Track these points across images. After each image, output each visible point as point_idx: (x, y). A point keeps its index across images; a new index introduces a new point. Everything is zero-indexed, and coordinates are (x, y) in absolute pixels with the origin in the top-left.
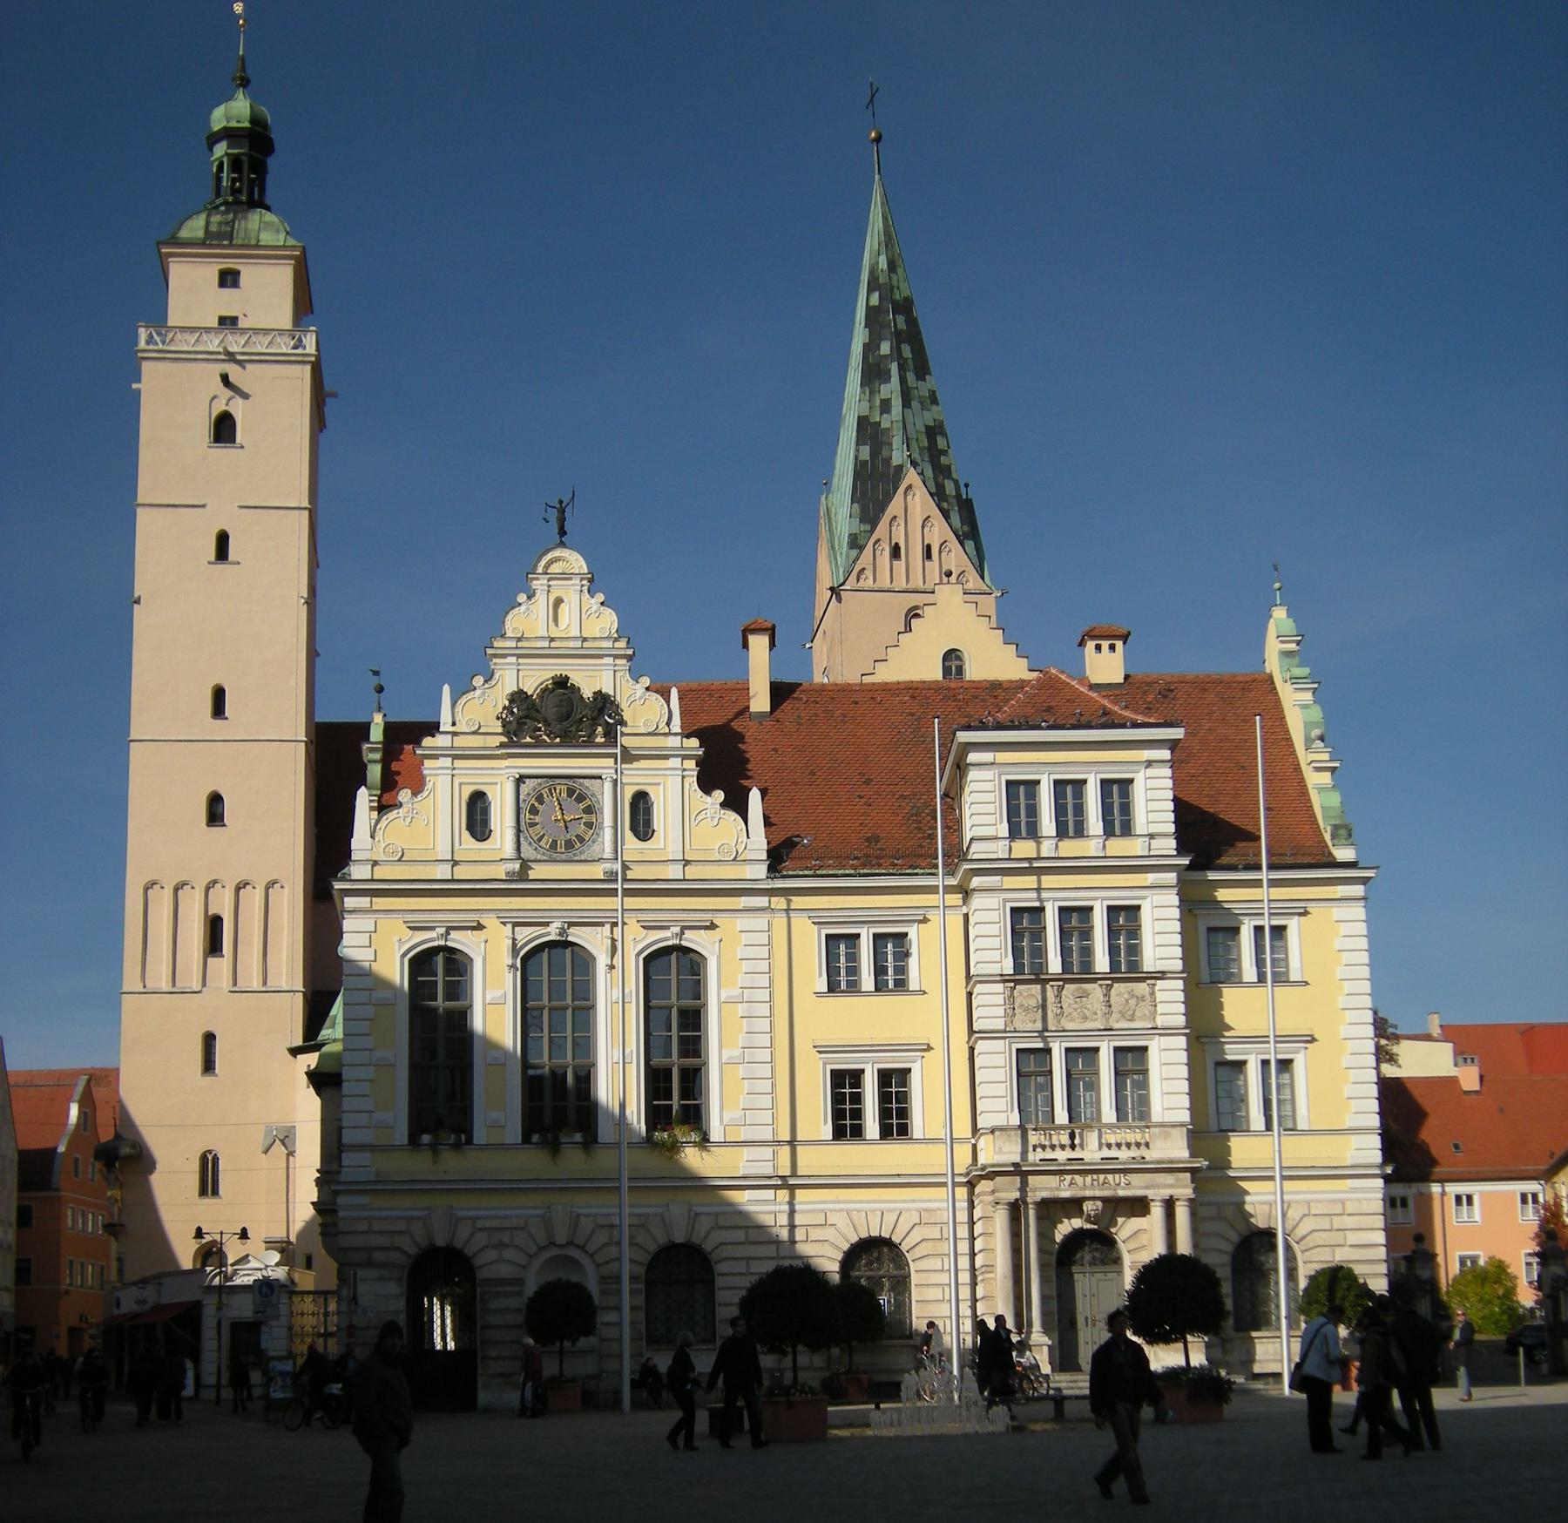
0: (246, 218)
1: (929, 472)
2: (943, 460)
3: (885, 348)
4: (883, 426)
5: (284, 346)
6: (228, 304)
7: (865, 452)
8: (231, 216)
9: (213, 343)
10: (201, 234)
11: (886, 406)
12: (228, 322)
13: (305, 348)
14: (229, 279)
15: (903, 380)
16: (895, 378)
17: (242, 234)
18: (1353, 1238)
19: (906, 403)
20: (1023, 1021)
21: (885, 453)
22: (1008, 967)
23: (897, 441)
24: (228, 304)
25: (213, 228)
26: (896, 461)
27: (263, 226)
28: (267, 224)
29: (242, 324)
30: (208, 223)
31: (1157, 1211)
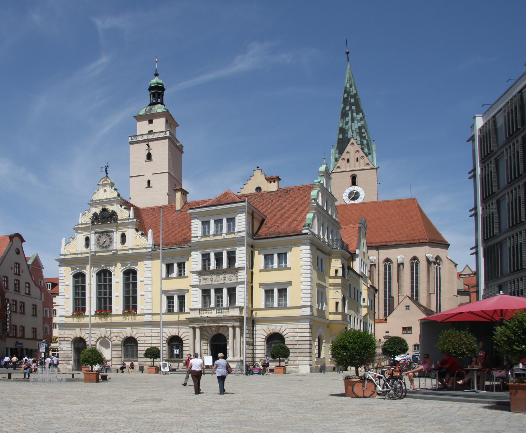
0: (154, 107)
1: (359, 138)
2: (363, 135)
3: (348, 108)
4: (346, 128)
5: (162, 135)
6: (151, 127)
7: (341, 136)
8: (151, 107)
9: (145, 138)
10: (144, 113)
11: (347, 123)
12: (151, 132)
13: (166, 135)
14: (151, 122)
15: (352, 116)
16: (350, 115)
17: (153, 110)
18: (300, 335)
19: (353, 121)
20: (203, 282)
21: (346, 136)
22: (199, 268)
23: (350, 132)
24: (151, 127)
25: (147, 111)
26: (349, 137)
27: (159, 109)
28: (159, 107)
29: (153, 132)
30: (146, 110)
31: (231, 330)
